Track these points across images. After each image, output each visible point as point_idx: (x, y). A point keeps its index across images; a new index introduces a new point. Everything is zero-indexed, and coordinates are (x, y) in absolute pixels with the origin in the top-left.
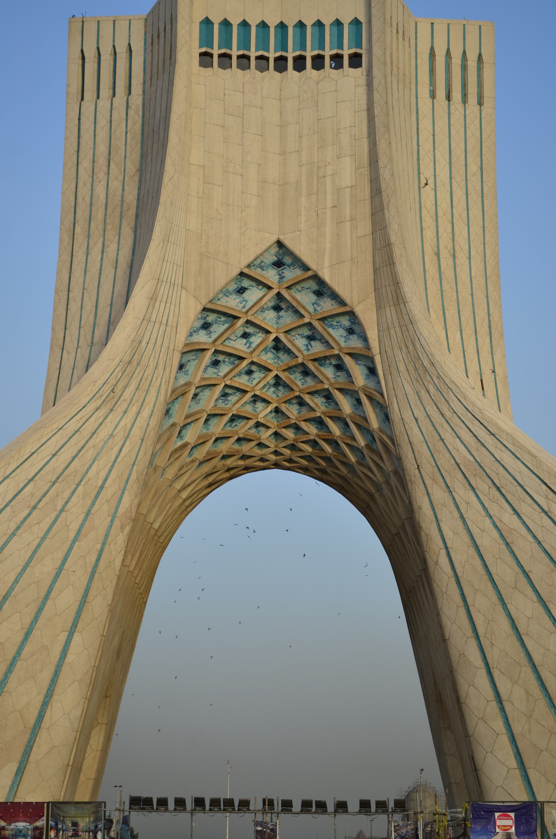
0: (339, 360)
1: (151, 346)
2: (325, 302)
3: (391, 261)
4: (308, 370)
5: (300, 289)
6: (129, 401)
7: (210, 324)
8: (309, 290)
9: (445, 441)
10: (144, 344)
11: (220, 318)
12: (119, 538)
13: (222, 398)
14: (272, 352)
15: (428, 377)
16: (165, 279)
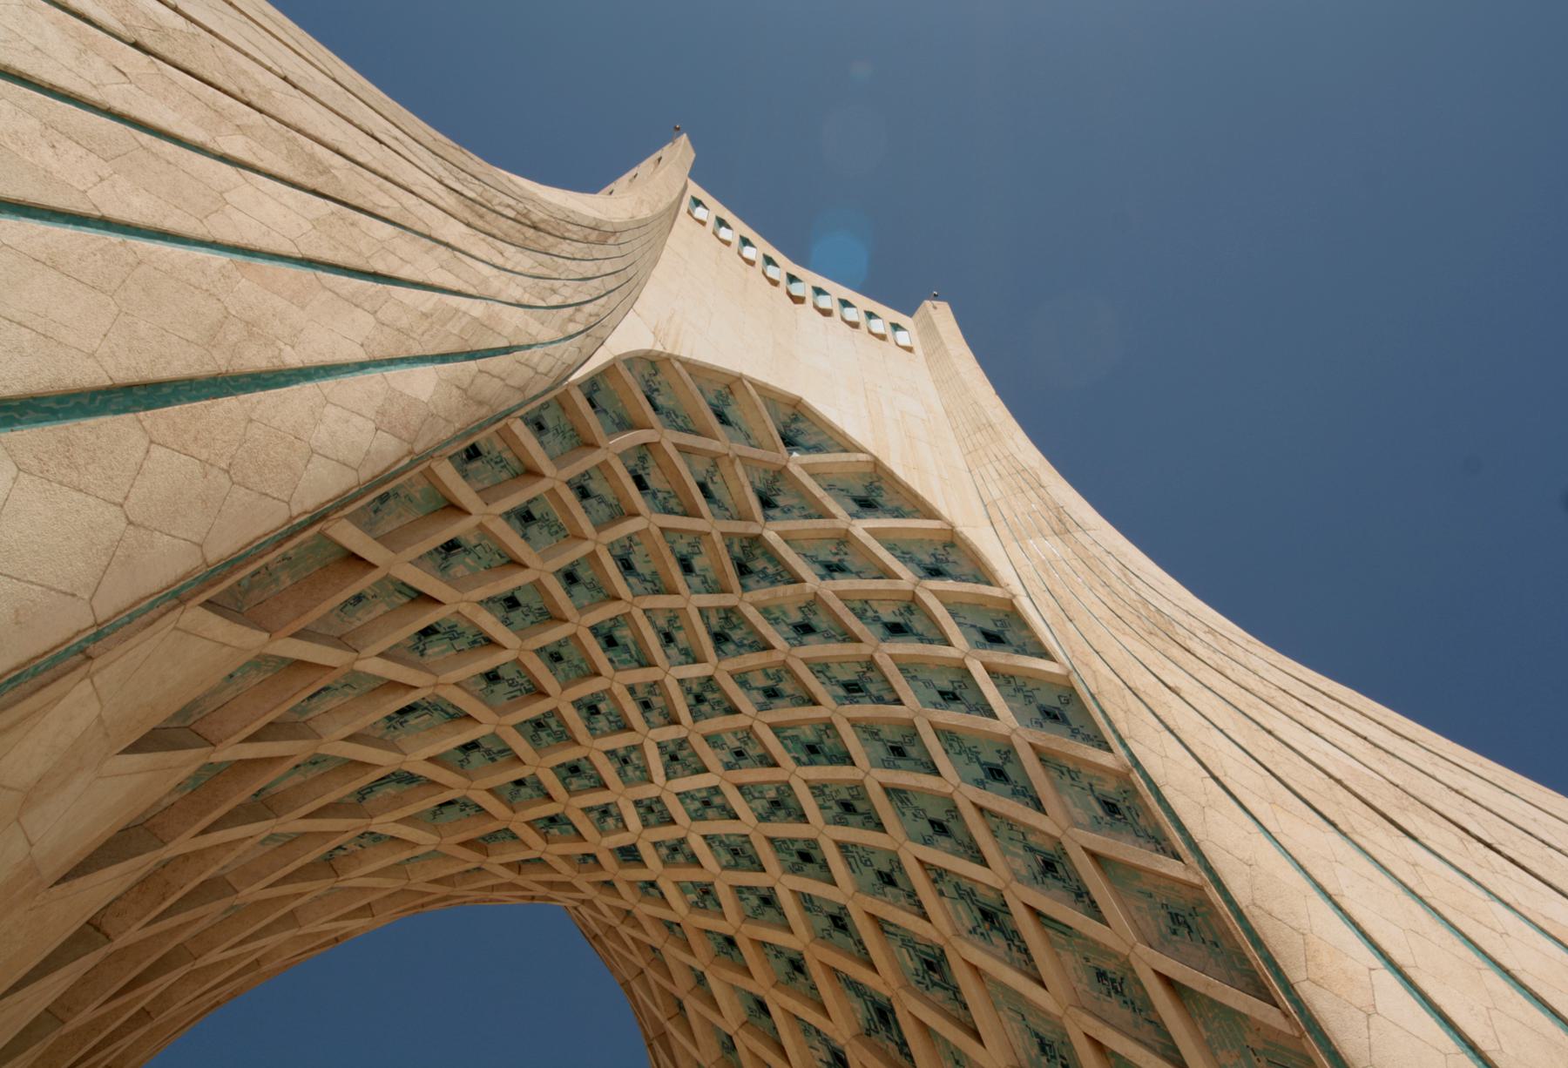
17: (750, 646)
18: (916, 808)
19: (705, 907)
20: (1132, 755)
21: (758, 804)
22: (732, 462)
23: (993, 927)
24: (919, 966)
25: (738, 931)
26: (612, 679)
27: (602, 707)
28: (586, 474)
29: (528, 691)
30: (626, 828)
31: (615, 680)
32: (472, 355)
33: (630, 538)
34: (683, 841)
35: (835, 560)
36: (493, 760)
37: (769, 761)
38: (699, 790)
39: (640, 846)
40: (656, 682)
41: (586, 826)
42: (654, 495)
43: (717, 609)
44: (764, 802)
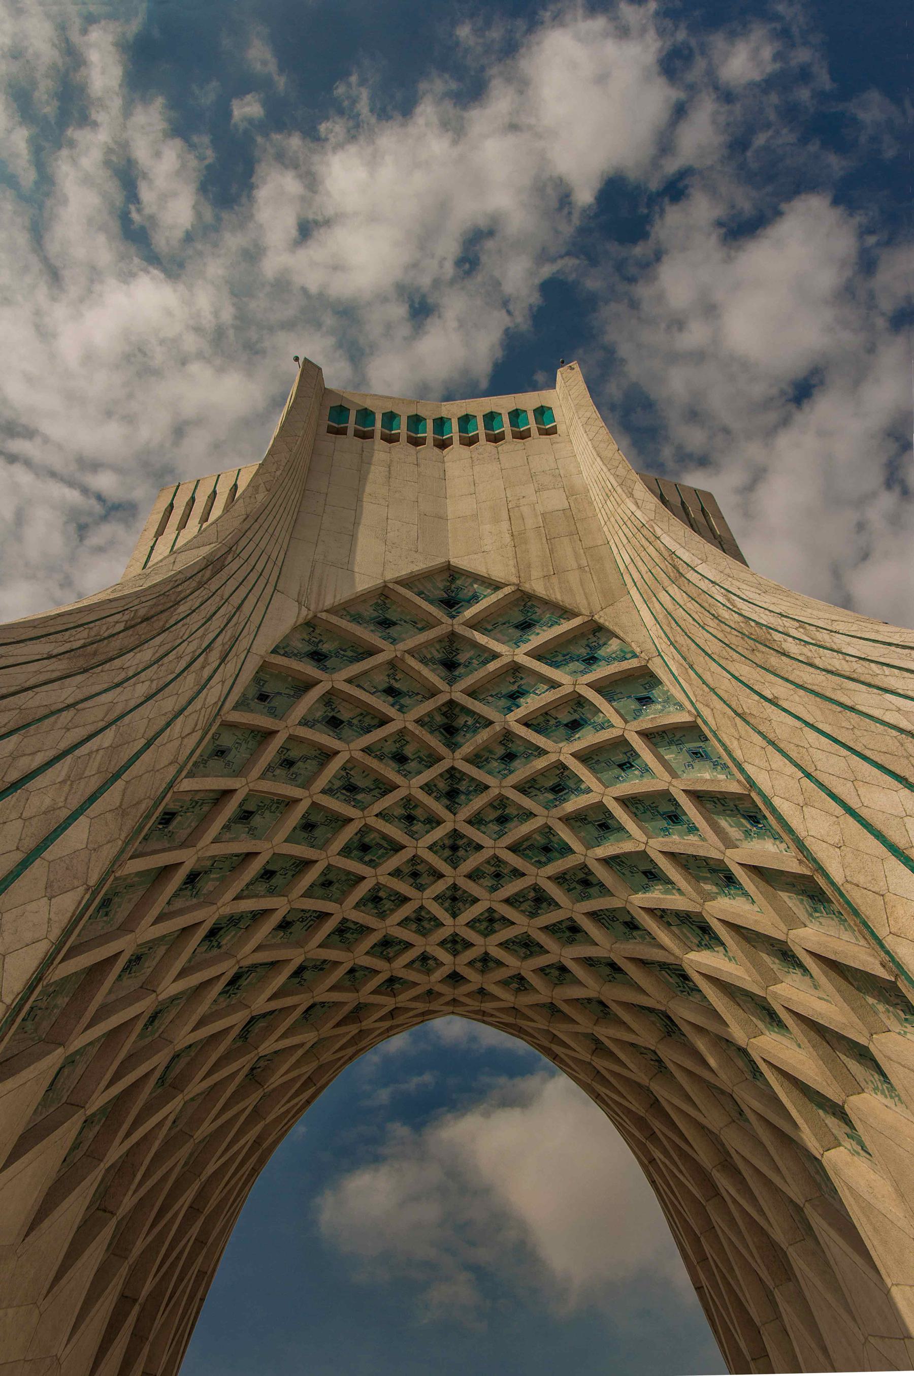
0: (575, 711)
1: (196, 619)
2: (538, 634)
3: (652, 539)
4: (513, 748)
5: (490, 628)
6: (131, 674)
7: (326, 657)
8: (507, 625)
9: (857, 707)
10: (183, 609)
11: (345, 651)
12: (32, 906)
13: (344, 791)
14: (440, 732)
15: (777, 636)
16: (245, 555)
17: (475, 791)
18: (630, 866)
19: (526, 989)
20: (748, 779)
21: (525, 906)
22: (403, 660)
23: (711, 938)
24: (678, 981)
25: (552, 998)
26: (376, 876)
27: (382, 894)
28: (284, 749)
29: (317, 918)
30: (443, 964)
31: (380, 875)
32: (116, 776)
33: (344, 768)
34: (486, 953)
35: (514, 688)
36: (322, 969)
37: (518, 874)
38: (482, 914)
39: (458, 970)
40: (414, 856)
41: (412, 976)
42: (350, 724)
43: (441, 775)
44: (529, 902)
